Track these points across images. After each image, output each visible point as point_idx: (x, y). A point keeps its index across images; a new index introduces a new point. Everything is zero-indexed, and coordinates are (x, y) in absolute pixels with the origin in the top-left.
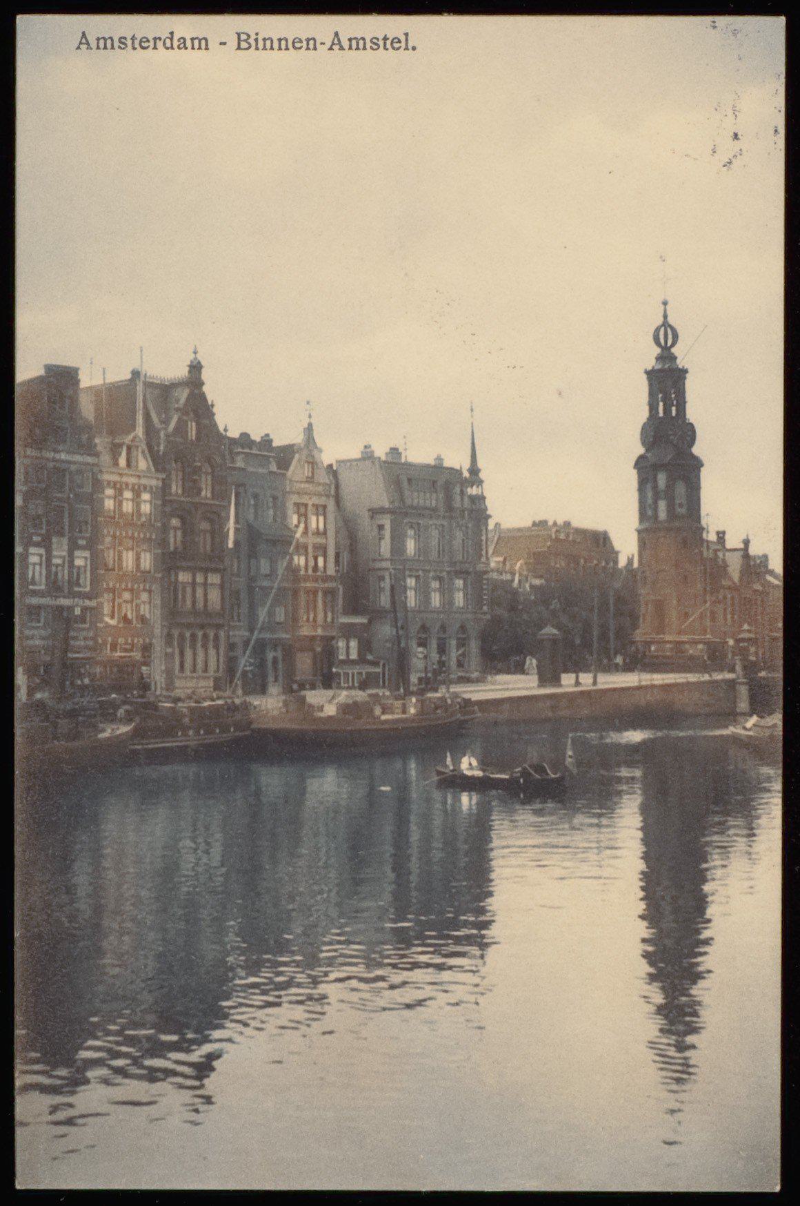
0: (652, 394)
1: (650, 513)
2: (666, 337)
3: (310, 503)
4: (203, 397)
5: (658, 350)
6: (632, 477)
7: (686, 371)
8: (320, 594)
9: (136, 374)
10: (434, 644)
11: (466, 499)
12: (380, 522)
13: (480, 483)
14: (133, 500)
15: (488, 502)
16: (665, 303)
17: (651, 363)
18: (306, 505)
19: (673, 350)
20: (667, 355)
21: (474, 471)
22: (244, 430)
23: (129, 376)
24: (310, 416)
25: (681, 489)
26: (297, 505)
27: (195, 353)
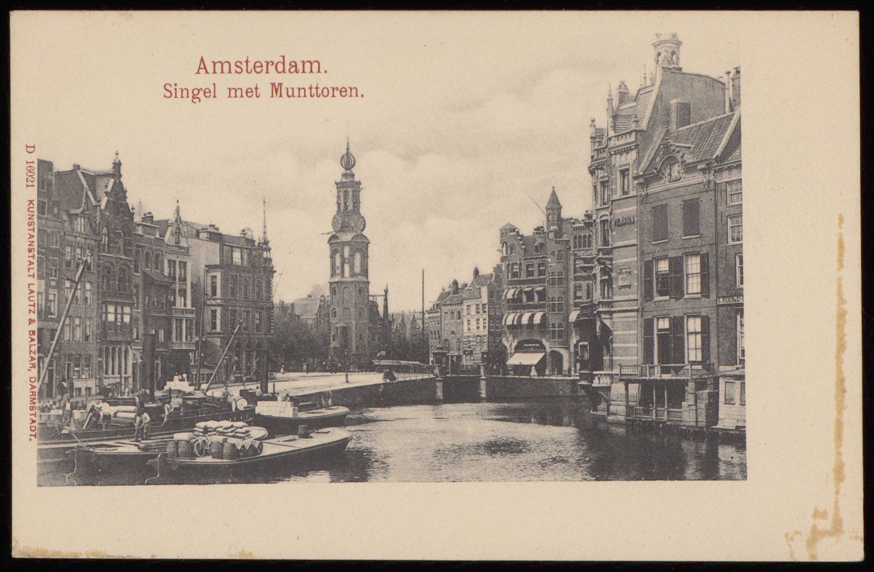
4: (121, 183)
5: (343, 170)
7: (359, 183)
8: (184, 322)
11: (262, 260)
15: (274, 263)
18: (175, 262)
19: (353, 170)
21: (266, 243)
23: (71, 168)
25: (358, 256)
26: (169, 261)
27: (117, 154)
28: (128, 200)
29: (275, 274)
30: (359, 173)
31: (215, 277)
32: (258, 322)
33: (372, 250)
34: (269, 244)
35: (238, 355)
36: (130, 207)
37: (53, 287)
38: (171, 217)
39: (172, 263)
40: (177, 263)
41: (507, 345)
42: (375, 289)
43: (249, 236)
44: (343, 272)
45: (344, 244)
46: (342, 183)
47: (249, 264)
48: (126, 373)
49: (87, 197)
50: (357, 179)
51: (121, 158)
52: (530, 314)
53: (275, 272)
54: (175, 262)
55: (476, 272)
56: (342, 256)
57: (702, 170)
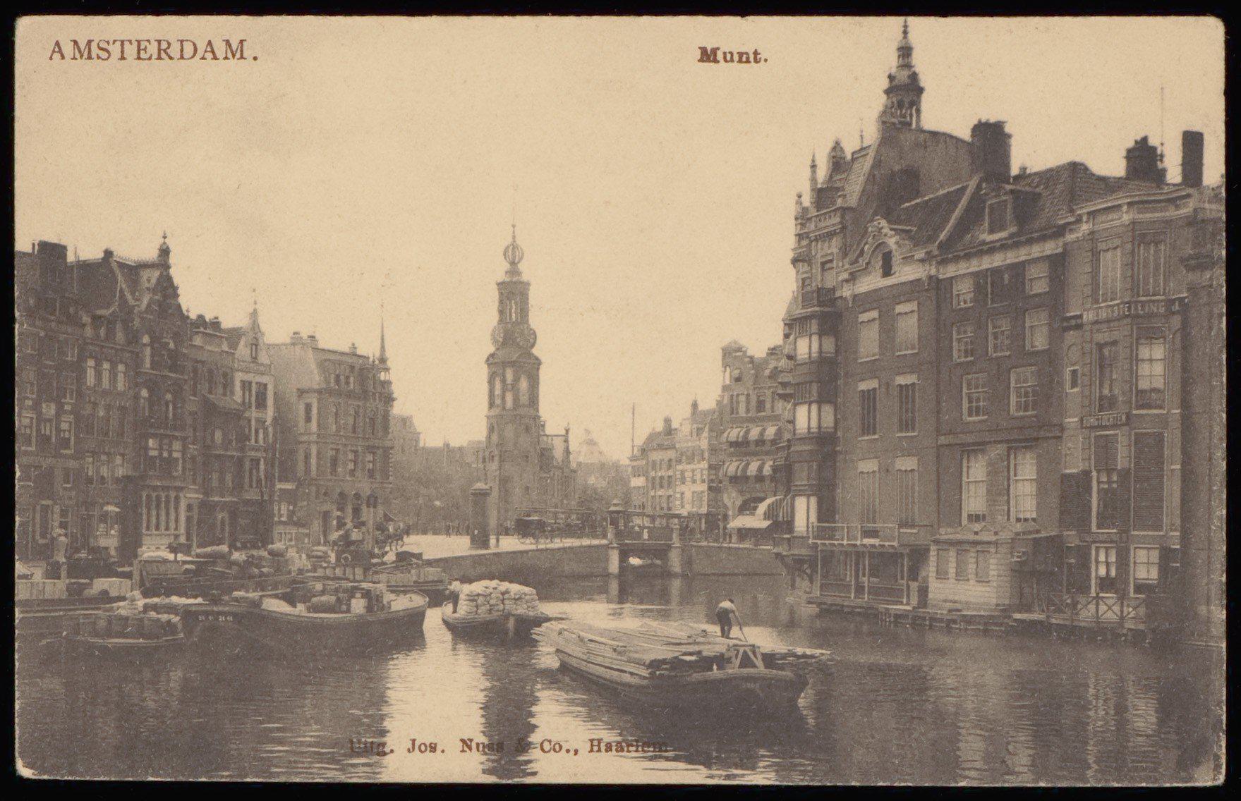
0: (501, 302)
1: (498, 401)
2: (513, 255)
4: (169, 278)
6: (484, 372)
9: (108, 254)
10: (349, 509)
12: (308, 401)
16: (514, 226)
17: (501, 276)
18: (250, 383)
20: (514, 270)
21: (383, 360)
22: (200, 313)
23: (101, 255)
25: (524, 384)
26: (243, 382)
27: (165, 237)
30: (527, 271)
32: (371, 466)
33: (545, 375)
35: (341, 509)
39: (246, 385)
41: (729, 505)
47: (359, 385)
48: (176, 529)
49: (122, 296)
50: (525, 278)
51: (171, 243)
52: (759, 463)
54: (250, 383)
55: (695, 405)
56: (504, 381)
57: (922, 261)
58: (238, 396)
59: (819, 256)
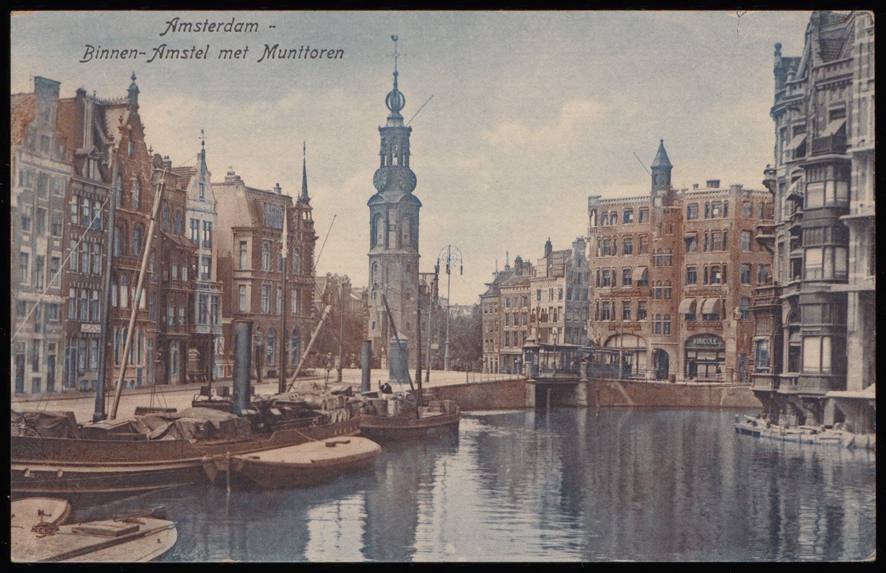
3: (201, 220)
4: (138, 118)
7: (410, 129)
8: (210, 299)
13: (309, 210)
14: (89, 208)
18: (198, 221)
21: (305, 199)
23: (74, 95)
24: (203, 143)
26: (192, 220)
28: (146, 139)
29: (317, 242)
31: (244, 243)
34: (310, 203)
36: (148, 148)
37: (56, 249)
38: (194, 163)
40: (201, 224)
42: (426, 266)
43: (284, 192)
44: (387, 239)
45: (389, 206)
46: (386, 128)
50: (406, 123)
53: (317, 238)
54: (198, 221)
55: (549, 245)
56: (387, 222)
58: (189, 233)
59: (827, 103)
